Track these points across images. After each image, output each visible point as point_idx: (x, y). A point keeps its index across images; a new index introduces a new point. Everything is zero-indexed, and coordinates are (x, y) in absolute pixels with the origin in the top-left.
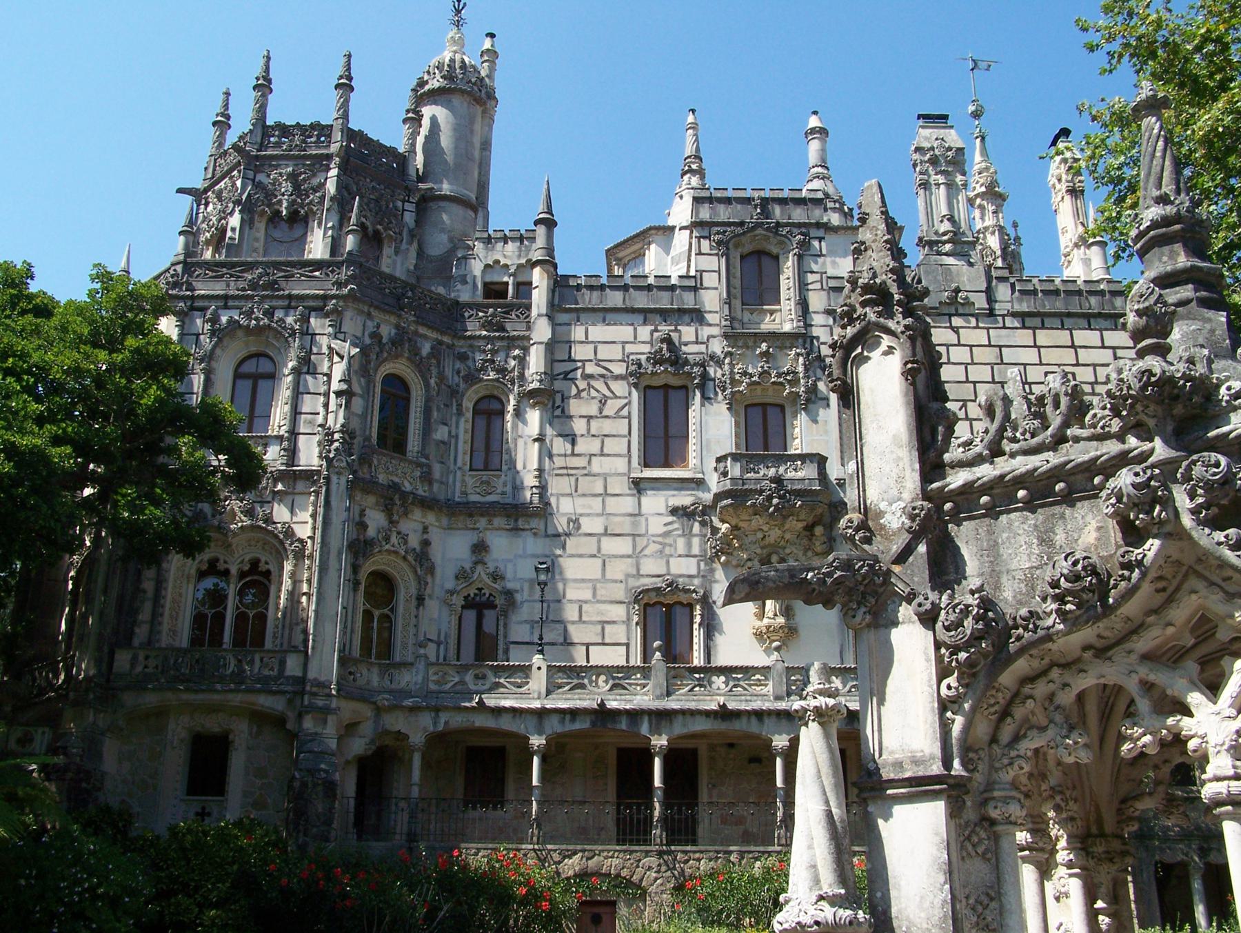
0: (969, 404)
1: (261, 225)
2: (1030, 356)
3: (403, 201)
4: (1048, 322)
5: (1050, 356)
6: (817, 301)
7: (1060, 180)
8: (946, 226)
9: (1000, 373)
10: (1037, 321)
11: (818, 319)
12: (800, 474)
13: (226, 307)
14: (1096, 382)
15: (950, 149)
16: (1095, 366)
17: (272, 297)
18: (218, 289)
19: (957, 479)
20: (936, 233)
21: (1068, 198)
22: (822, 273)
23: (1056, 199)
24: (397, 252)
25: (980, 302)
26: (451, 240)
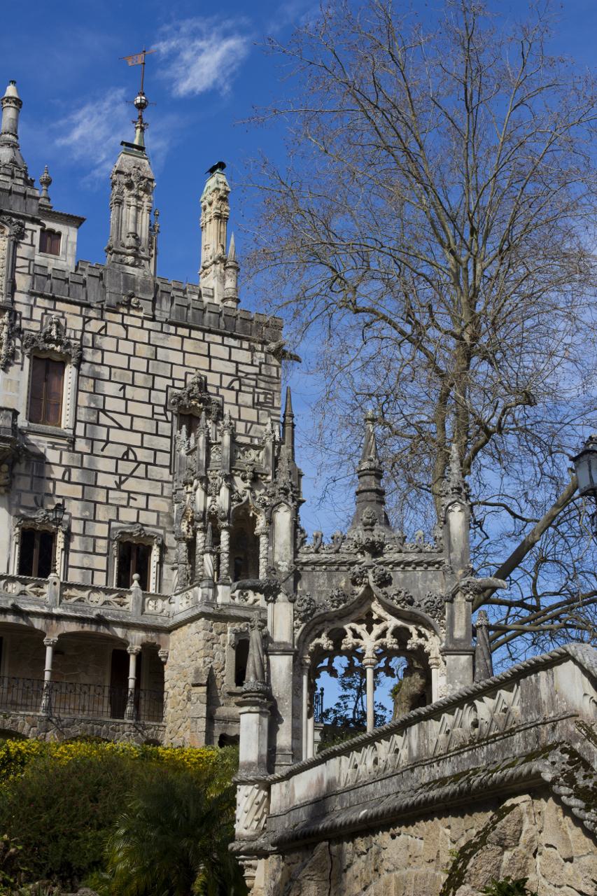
0: (127, 386)
2: (176, 357)
4: (195, 334)
5: (193, 361)
6: (22, 282)
7: (210, 204)
8: (130, 241)
9: (153, 367)
10: (185, 332)
11: (19, 297)
14: (221, 387)
15: (143, 178)
16: (222, 374)
19: (304, 558)
20: (123, 246)
21: (214, 222)
22: (30, 261)
23: (205, 218)
25: (147, 307)
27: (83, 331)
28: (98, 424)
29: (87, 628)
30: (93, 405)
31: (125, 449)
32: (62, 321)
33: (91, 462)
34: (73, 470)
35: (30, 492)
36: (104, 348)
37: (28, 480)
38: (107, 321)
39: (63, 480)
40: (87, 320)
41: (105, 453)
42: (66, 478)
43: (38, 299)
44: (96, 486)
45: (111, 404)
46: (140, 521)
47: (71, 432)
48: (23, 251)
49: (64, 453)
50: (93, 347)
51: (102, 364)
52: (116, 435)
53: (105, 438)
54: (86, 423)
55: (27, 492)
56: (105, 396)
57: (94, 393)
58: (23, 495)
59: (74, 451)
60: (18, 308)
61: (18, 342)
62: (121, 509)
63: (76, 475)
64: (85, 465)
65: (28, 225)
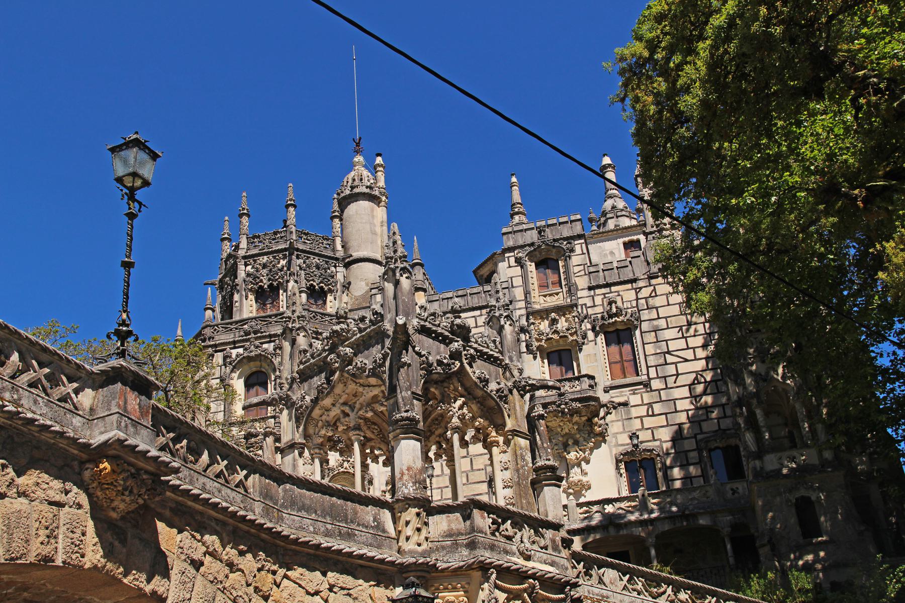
1: (251, 297)
3: (335, 267)
6: (582, 282)
12: (578, 388)
13: (235, 348)
17: (260, 338)
18: (229, 337)
24: (335, 299)
26: (367, 285)
27: (637, 299)
28: (666, 364)
29: (678, 525)
30: (658, 351)
31: (694, 375)
32: (619, 299)
33: (667, 395)
34: (654, 405)
35: (624, 432)
36: (657, 305)
37: (620, 423)
38: (654, 286)
39: (648, 415)
40: (638, 290)
41: (678, 384)
42: (650, 413)
43: (598, 291)
44: (676, 411)
45: (672, 346)
46: (722, 427)
47: (646, 377)
48: (575, 260)
49: (644, 395)
50: (648, 308)
51: (659, 318)
52: (682, 368)
53: (675, 373)
54: (656, 366)
55: (621, 433)
56: (666, 341)
57: (658, 342)
58: (618, 436)
59: (652, 391)
60: (581, 302)
61: (589, 326)
62: (702, 423)
63: (657, 408)
64: (663, 398)
65: (576, 242)
